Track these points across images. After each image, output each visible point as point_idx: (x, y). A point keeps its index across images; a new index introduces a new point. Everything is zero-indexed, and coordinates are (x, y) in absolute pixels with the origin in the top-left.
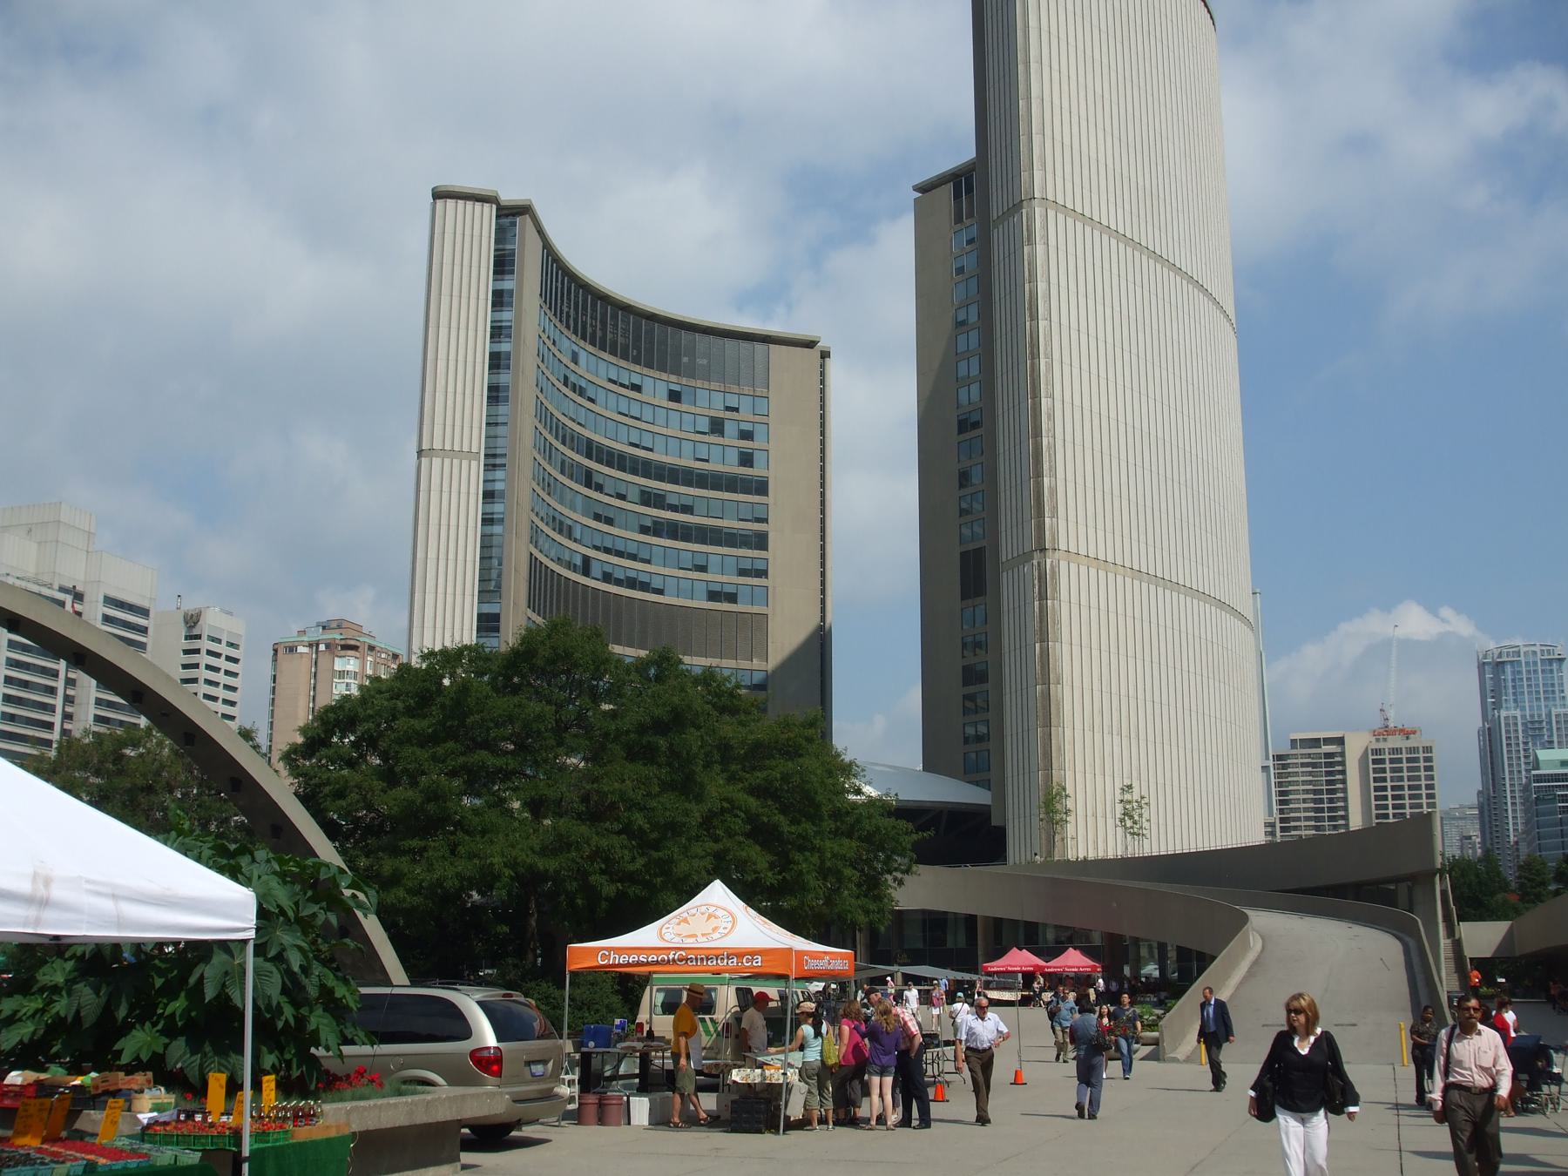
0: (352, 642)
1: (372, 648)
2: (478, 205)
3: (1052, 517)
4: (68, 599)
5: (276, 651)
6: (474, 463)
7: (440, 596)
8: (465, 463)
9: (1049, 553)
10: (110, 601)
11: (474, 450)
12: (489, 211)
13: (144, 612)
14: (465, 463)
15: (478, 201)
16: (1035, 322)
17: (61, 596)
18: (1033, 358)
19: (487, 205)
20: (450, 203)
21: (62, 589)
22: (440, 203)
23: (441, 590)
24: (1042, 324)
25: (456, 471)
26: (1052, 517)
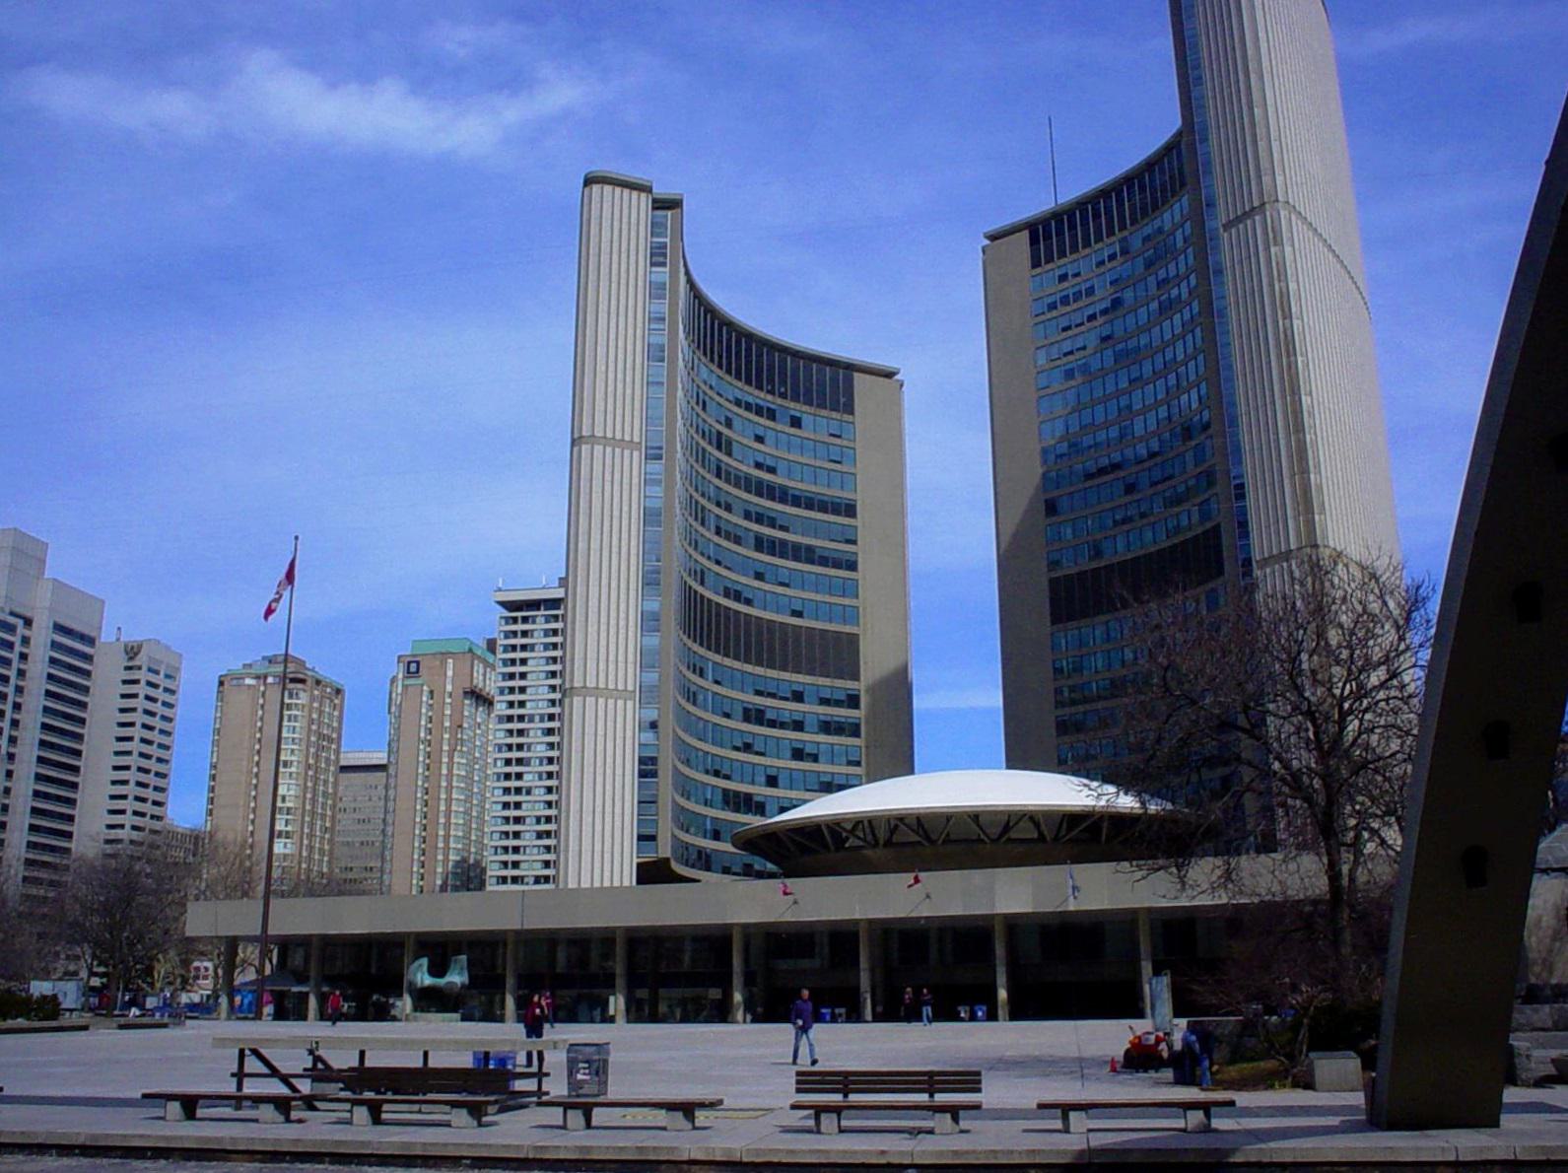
0: (301, 676)
1: (318, 682)
2: (635, 194)
3: (1320, 514)
4: (20, 623)
5: (221, 683)
6: (636, 454)
7: (604, 590)
8: (627, 453)
9: (1321, 549)
10: (59, 628)
11: (636, 439)
12: (645, 200)
13: (90, 641)
14: (627, 453)
15: (635, 189)
16: (1287, 321)
17: (12, 620)
18: (1288, 356)
19: (643, 195)
20: (608, 188)
21: (12, 614)
22: (596, 188)
23: (605, 581)
24: (1296, 322)
25: (617, 461)
26: (1320, 514)
